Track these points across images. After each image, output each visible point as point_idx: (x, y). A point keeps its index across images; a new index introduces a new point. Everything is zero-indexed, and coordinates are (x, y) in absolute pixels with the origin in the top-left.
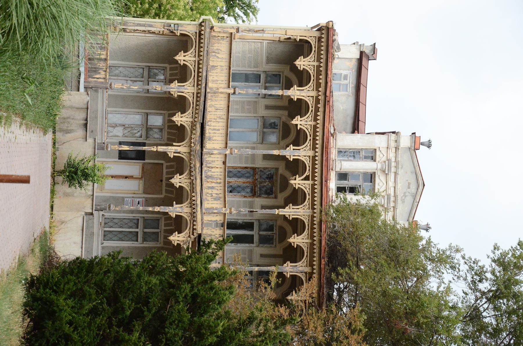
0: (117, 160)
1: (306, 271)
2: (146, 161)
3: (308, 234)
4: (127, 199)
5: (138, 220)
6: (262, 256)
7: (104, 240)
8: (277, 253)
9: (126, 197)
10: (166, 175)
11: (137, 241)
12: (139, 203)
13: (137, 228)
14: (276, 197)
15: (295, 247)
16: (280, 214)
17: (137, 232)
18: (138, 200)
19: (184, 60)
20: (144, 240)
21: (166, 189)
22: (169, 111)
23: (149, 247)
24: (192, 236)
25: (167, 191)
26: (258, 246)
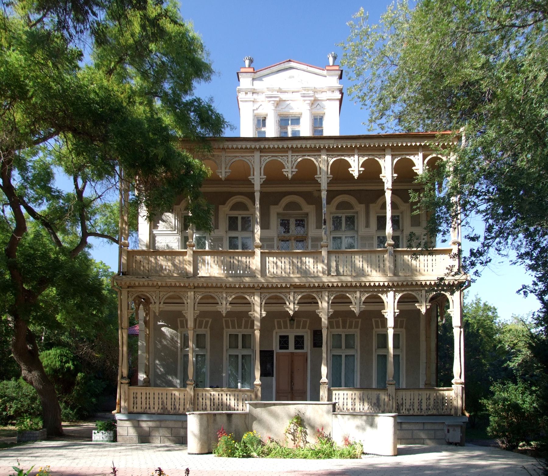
0: (274, 379)
2: (274, 349)
5: (333, 355)
11: (354, 356)
13: (341, 356)
14: (307, 214)
20: (353, 347)
22: (223, 328)
26: (357, 232)
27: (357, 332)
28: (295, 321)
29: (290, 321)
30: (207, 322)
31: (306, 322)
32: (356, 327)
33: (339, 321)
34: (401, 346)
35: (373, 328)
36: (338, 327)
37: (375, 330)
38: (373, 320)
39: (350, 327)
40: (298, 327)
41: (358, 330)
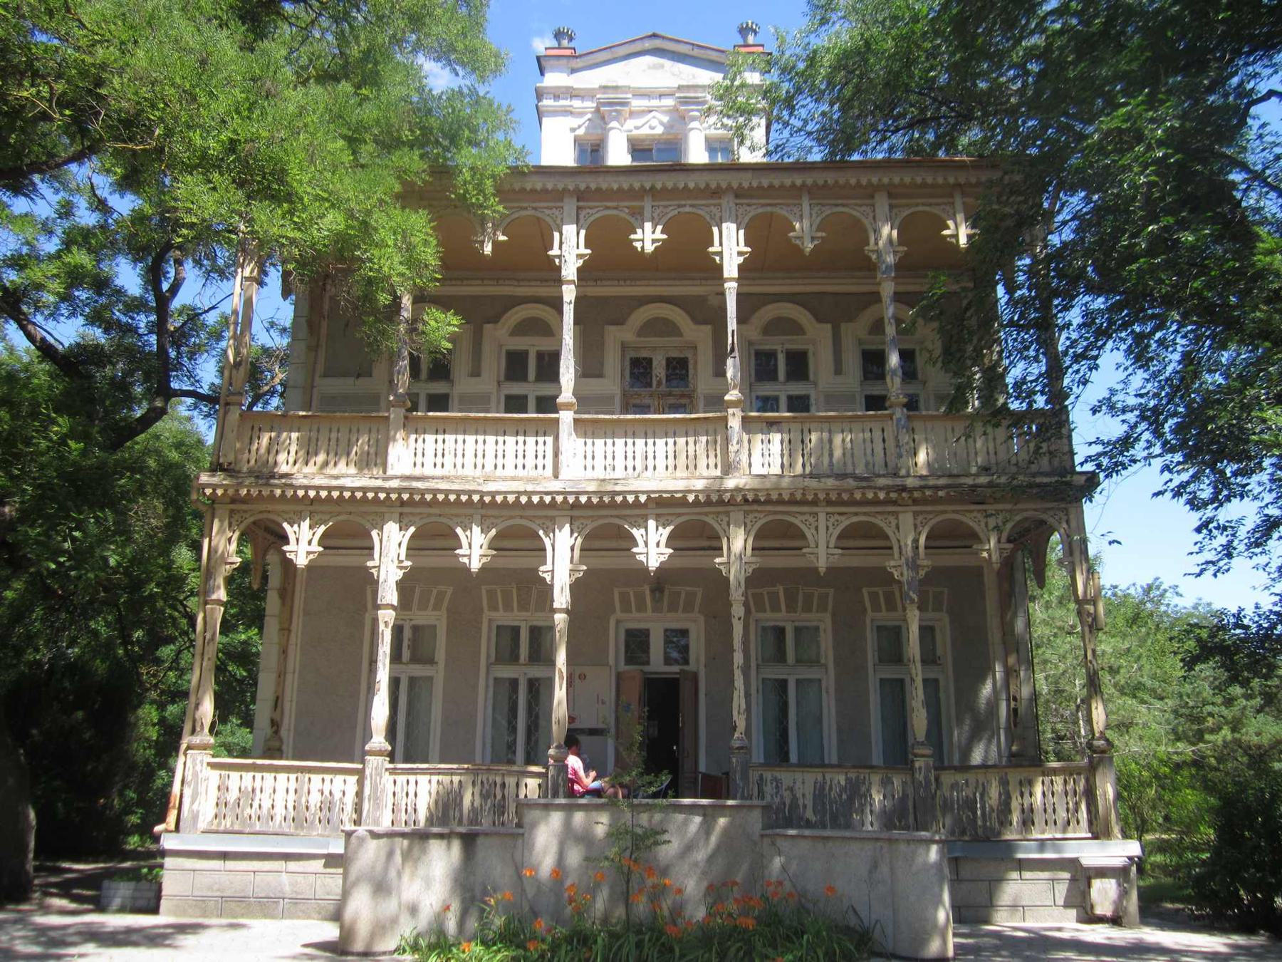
1: (887, 208)
3: (788, 205)
6: (838, 371)
8: (829, 334)
10: (646, 611)
19: (310, 543)
20: (815, 662)
22: (482, 609)
26: (815, 384)
28: (666, 592)
29: (653, 591)
30: (441, 595)
32: (822, 608)
34: (939, 652)
38: (865, 591)
39: (807, 608)
40: (673, 607)
41: (828, 618)
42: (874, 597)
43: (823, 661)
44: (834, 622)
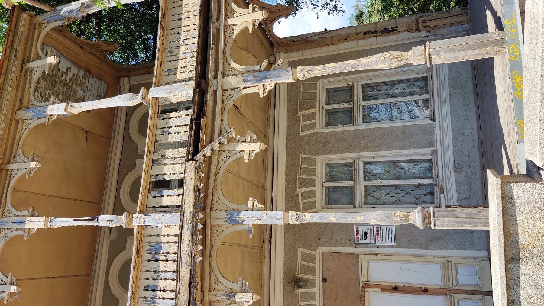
4: (389, 242)
5: (365, 203)
7: (430, 161)
9: (392, 246)
11: (365, 163)
12: (366, 234)
15: (251, 199)
16: (43, 218)
17: (365, 179)
18: (368, 241)
20: (351, 166)
21: (314, 262)
23: (342, 153)
24: (209, 154)
25: (313, 259)
27: (321, 162)
31: (302, 254)
32: (313, 162)
33: (303, 193)
34: (344, 85)
35: (316, 133)
36: (312, 194)
37: (318, 129)
38: (302, 134)
39: (313, 172)
41: (320, 158)
42: (305, 128)
43: (351, 161)
44: (323, 153)
